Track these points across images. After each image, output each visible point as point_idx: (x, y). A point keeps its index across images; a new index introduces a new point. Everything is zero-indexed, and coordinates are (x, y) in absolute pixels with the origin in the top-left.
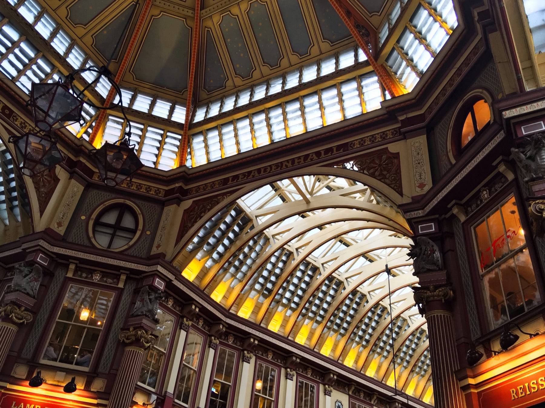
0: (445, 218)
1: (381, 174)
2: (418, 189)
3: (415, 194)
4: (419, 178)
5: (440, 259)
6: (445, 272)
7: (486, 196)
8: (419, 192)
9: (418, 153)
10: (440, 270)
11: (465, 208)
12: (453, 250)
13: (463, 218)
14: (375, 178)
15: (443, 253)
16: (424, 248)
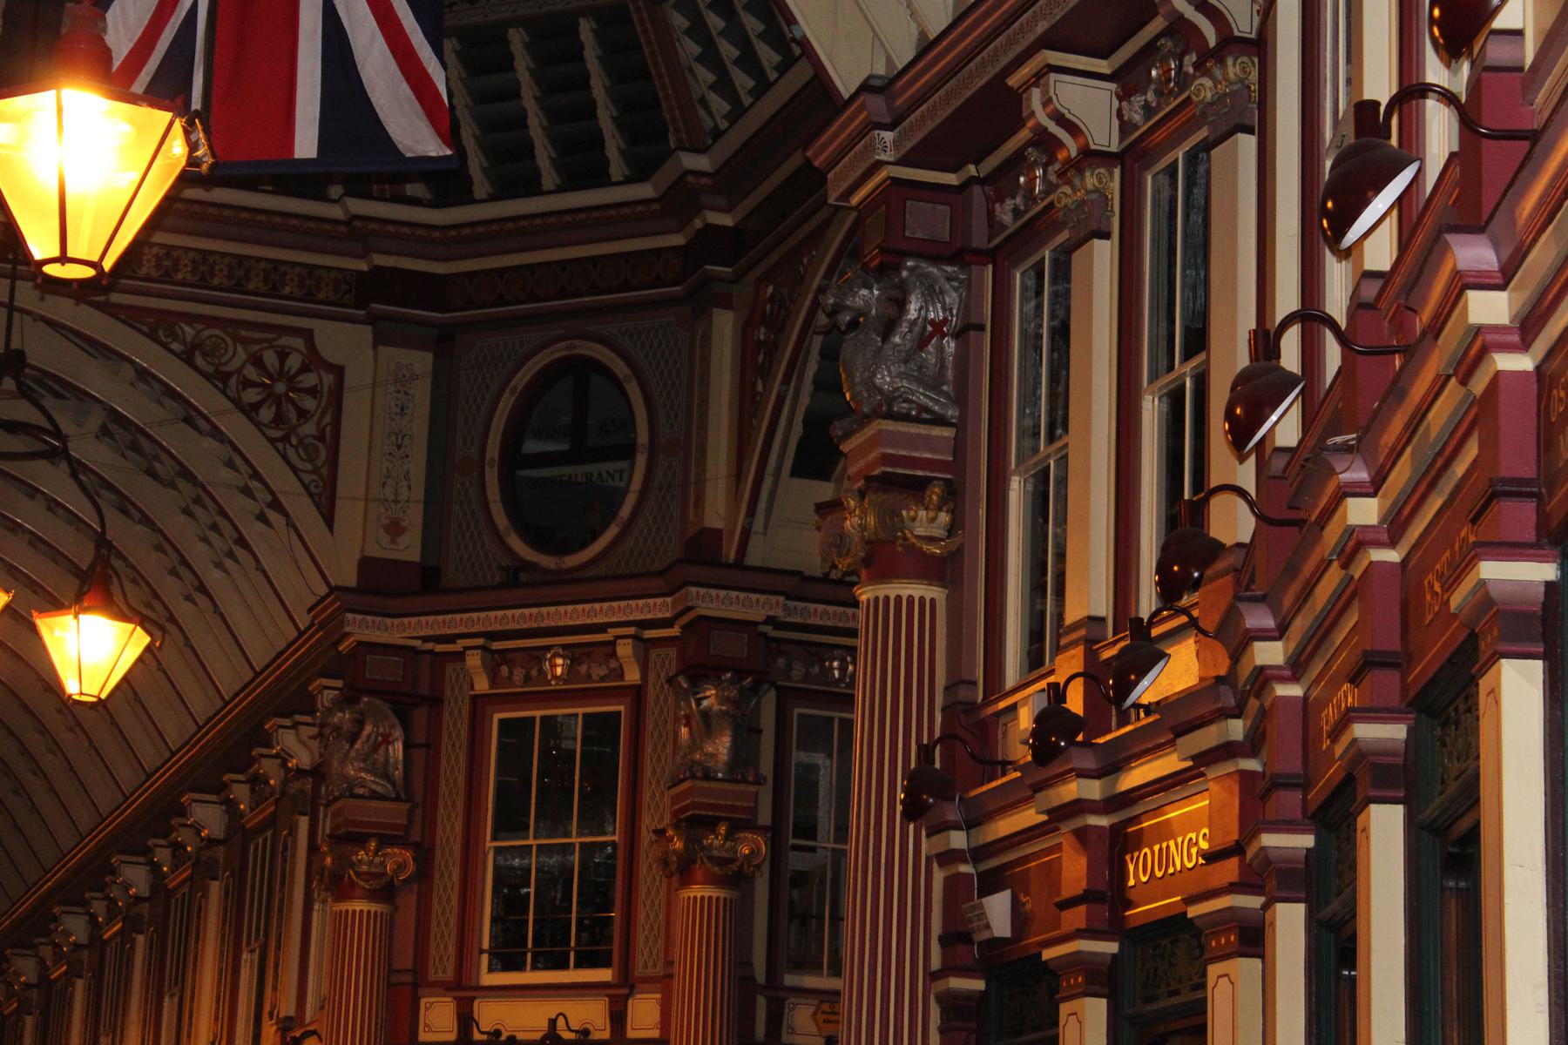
0: (431, 652)
1: (278, 420)
2: (385, 539)
3: (373, 551)
4: (393, 497)
5: (400, 767)
6: (408, 805)
7: (559, 671)
8: (381, 548)
9: (402, 409)
10: (398, 799)
11: (496, 662)
12: (432, 747)
13: (482, 685)
14: (258, 424)
15: (407, 747)
16: (368, 728)
